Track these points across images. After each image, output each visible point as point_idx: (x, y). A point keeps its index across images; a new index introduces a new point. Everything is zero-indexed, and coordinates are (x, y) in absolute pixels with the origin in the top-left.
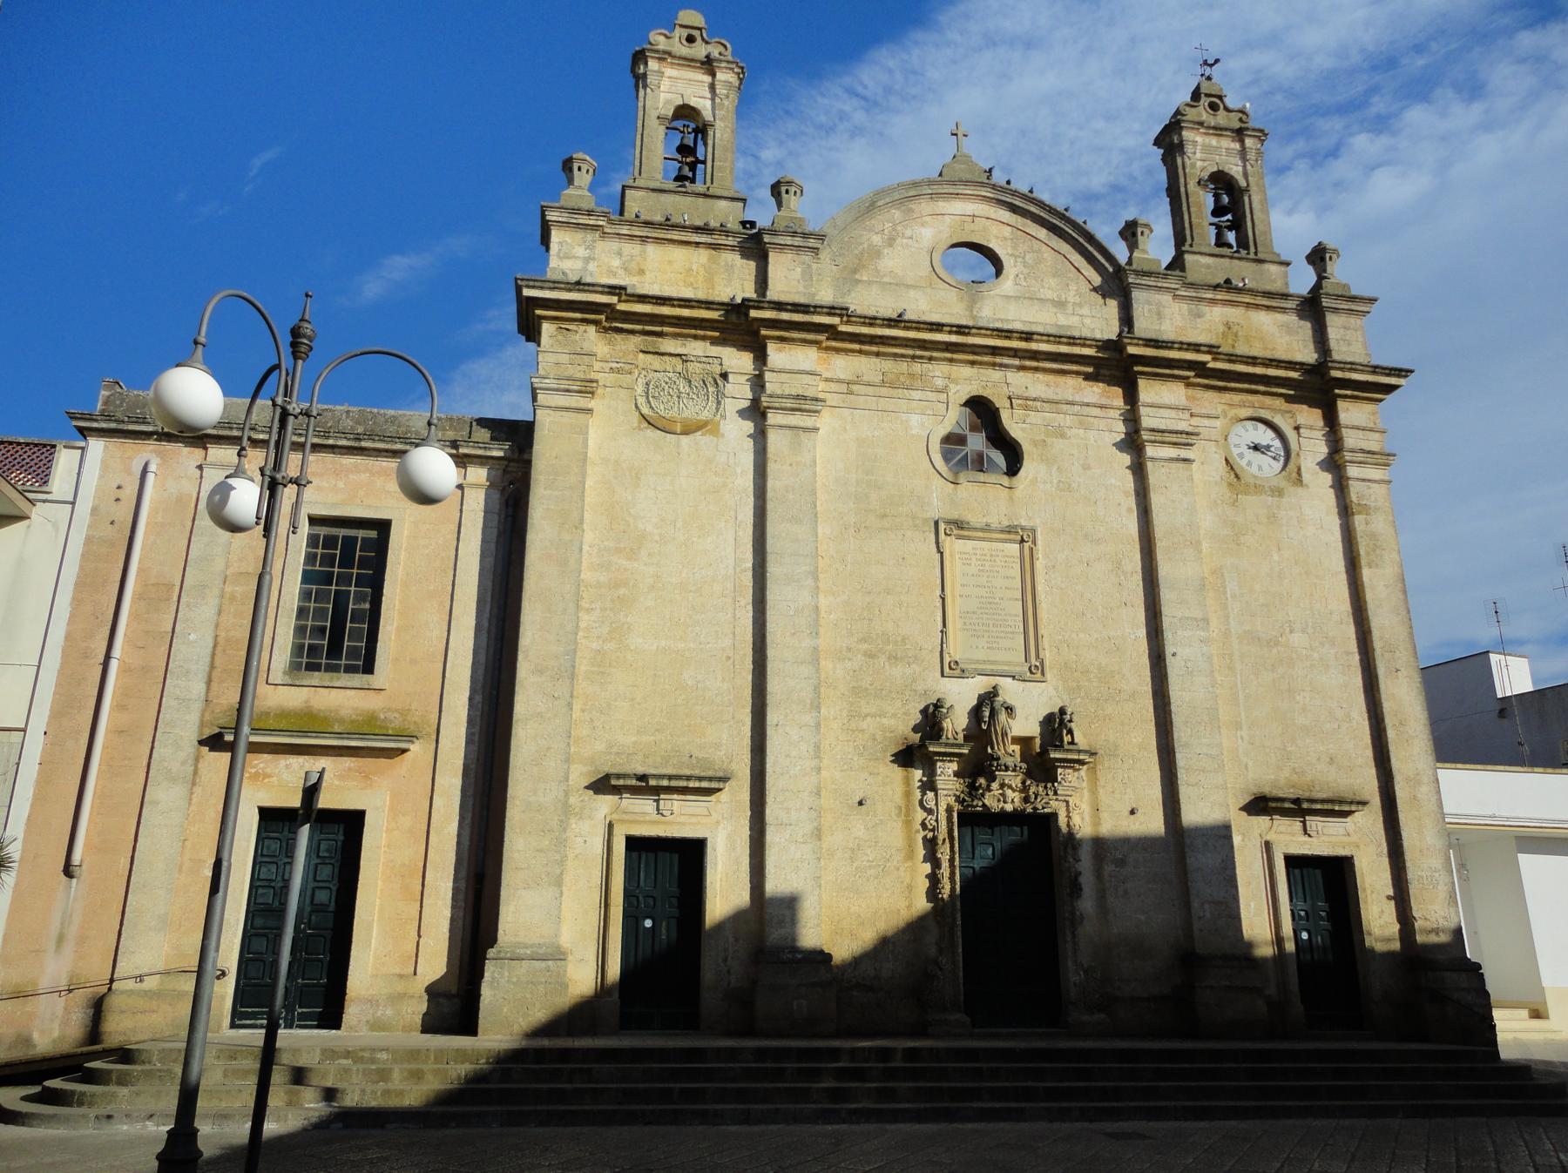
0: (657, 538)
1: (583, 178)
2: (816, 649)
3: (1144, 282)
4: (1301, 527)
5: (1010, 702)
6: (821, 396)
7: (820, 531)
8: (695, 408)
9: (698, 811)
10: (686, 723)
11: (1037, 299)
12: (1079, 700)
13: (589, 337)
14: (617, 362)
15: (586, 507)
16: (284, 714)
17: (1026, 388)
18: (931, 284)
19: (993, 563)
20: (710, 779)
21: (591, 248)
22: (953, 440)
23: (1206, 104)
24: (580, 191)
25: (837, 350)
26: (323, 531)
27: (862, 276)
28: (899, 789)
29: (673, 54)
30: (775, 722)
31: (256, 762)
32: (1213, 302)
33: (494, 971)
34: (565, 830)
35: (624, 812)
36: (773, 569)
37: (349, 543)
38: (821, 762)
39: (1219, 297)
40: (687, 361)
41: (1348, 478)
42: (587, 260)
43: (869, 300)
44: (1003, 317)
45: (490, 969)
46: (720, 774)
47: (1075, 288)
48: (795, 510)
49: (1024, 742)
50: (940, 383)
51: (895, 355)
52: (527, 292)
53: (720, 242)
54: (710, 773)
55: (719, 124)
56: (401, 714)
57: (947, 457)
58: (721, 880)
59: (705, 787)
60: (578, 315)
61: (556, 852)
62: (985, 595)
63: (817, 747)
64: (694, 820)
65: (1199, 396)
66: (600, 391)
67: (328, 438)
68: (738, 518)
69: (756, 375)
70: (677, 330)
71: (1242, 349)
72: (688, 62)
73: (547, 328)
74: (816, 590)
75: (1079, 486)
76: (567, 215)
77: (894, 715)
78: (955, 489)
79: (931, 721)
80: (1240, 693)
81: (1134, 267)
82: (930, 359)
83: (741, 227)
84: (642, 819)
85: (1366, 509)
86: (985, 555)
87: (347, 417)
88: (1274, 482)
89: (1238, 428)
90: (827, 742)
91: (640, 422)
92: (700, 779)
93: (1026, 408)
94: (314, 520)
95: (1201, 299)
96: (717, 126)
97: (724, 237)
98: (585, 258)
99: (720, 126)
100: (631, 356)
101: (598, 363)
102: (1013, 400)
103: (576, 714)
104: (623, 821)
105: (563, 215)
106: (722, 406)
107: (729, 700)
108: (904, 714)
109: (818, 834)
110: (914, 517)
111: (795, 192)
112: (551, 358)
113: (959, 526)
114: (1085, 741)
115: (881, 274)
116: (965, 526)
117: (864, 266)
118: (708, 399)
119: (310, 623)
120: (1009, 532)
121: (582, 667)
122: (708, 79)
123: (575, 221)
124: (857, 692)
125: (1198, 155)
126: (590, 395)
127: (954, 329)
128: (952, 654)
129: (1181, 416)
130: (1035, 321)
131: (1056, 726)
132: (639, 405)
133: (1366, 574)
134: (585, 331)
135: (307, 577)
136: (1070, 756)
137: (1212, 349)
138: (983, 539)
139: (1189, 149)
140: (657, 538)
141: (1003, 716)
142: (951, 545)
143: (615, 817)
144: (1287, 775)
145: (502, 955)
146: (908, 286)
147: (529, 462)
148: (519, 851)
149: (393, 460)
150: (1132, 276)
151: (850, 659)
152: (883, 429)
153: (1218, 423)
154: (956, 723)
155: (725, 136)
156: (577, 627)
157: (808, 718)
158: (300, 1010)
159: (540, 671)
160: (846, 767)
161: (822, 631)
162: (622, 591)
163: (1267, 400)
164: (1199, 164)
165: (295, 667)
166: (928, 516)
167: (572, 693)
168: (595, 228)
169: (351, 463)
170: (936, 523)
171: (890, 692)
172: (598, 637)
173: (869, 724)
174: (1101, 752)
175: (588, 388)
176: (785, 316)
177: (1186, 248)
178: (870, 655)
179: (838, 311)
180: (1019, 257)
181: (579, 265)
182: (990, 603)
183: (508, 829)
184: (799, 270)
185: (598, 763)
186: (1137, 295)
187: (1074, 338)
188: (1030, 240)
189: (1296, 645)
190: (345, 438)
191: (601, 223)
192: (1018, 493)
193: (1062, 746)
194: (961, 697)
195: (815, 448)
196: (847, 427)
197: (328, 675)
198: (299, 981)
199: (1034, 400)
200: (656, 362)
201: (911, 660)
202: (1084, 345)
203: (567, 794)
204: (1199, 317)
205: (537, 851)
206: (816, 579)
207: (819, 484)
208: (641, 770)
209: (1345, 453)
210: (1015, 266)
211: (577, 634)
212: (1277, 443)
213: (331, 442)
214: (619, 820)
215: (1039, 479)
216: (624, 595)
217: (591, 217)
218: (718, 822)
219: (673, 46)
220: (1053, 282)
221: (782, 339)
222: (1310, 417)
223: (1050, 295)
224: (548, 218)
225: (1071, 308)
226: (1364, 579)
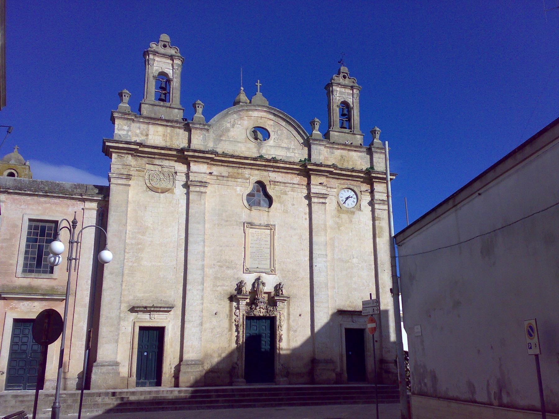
0: (152, 228)
1: (126, 99)
2: (203, 265)
3: (315, 142)
4: (359, 224)
5: (264, 281)
6: (208, 181)
7: (206, 226)
8: (165, 185)
9: (163, 318)
10: (160, 289)
11: (281, 147)
12: (286, 280)
13: (129, 159)
14: (139, 168)
15: (128, 218)
16: (22, 287)
17: (275, 178)
18: (246, 141)
19: (261, 236)
20: (168, 307)
21: (129, 126)
22: (250, 195)
23: (342, 76)
24: (124, 105)
25: (214, 165)
26: (34, 224)
27: (223, 138)
28: (227, 309)
29: (159, 52)
30: (189, 289)
31: (12, 304)
32: (338, 149)
33: (96, 370)
34: (119, 325)
35: (139, 319)
36: (190, 239)
37: (43, 228)
38: (203, 301)
39: (339, 147)
40: (163, 167)
41: (375, 209)
42: (128, 131)
43: (223, 147)
44: (269, 153)
45: (94, 370)
46: (171, 306)
47: (293, 143)
48: (198, 220)
49: (269, 293)
50: (247, 176)
51: (233, 167)
52: (107, 144)
53: (174, 125)
54: (167, 306)
55: (175, 80)
56: (62, 287)
57: (248, 201)
58: (170, 340)
59: (167, 309)
60: (125, 152)
61: (116, 332)
62: (258, 247)
63: (202, 297)
64: (162, 320)
65: (330, 181)
66: (133, 177)
67: (36, 192)
68: (180, 222)
69: (187, 173)
70: (160, 157)
71: (345, 166)
72: (164, 55)
73: (114, 155)
74: (204, 246)
75: (290, 211)
76: (121, 115)
77: (227, 286)
78: (250, 212)
79: (239, 288)
80: (336, 278)
81: (313, 137)
82: (245, 168)
83: (182, 120)
84: (144, 321)
85: (379, 219)
86: (259, 234)
87: (42, 184)
88: (352, 210)
89: (343, 192)
90: (206, 294)
91: (146, 189)
92: (164, 307)
93: (275, 185)
94: (30, 220)
95: (333, 148)
96: (174, 81)
97: (176, 124)
98: (127, 130)
99: (175, 80)
100: (144, 165)
101: (132, 168)
102: (271, 182)
103: (124, 287)
104: (138, 322)
105: (120, 114)
106: (175, 184)
107: (175, 282)
108: (231, 285)
109: (201, 324)
110: (237, 221)
111: (201, 107)
112: (116, 166)
113: (251, 225)
114: (287, 293)
115: (230, 137)
116: (253, 224)
117: (224, 135)
118: (170, 181)
119: (29, 256)
120: (267, 226)
121: (126, 272)
122: (171, 62)
123: (124, 117)
124: (216, 278)
125: (338, 95)
126: (129, 180)
127: (252, 159)
128: (247, 266)
129: (324, 188)
130: (279, 155)
131: (278, 288)
132: (146, 183)
133: (378, 240)
134: (127, 157)
135: (28, 240)
136: (281, 299)
137: (334, 166)
138: (259, 229)
139: (335, 93)
140: (152, 228)
141: (261, 286)
142: (249, 231)
143: (135, 320)
144: (348, 303)
145: (98, 365)
146: (238, 142)
147: (108, 201)
148: (104, 332)
149: (59, 199)
150: (312, 140)
151: (214, 268)
152: (228, 192)
153: (336, 190)
154: (248, 288)
155: (176, 85)
156: (124, 258)
157: (200, 287)
158: (28, 384)
159: (111, 273)
160: (211, 302)
161: (205, 259)
162: (140, 246)
163: (352, 182)
164: (338, 98)
165: (24, 271)
166: (241, 221)
167: (122, 281)
168: (130, 119)
169: (43, 200)
170: (244, 223)
171: (226, 278)
172: (131, 262)
173: (219, 289)
174: (291, 297)
175: (129, 177)
176: (197, 154)
177: (331, 129)
178: (221, 267)
179: (214, 153)
180: (276, 132)
181: (125, 133)
182: (258, 251)
183: (100, 325)
184: (202, 136)
185: (130, 303)
186: (312, 146)
187: (291, 163)
188: (280, 126)
189: (354, 262)
190: (42, 192)
191: (133, 118)
192: (270, 213)
193: (279, 295)
194: (249, 280)
195: (205, 198)
196: (216, 191)
197: (37, 274)
198: (28, 375)
199: (277, 182)
200: (151, 167)
201: (234, 268)
202: (294, 165)
203: (120, 313)
204: (333, 154)
205: (110, 332)
206: (204, 242)
207: (206, 211)
208: (145, 305)
209: (374, 201)
210: (274, 135)
211: (124, 261)
212: (355, 196)
213: (36, 193)
214: (137, 321)
215: (277, 209)
216: (140, 247)
217: (129, 116)
218: (169, 321)
219: (158, 48)
220: (286, 141)
221: (195, 161)
222: (365, 187)
223: (285, 145)
224: (114, 115)
225: (292, 150)
226: (377, 241)
